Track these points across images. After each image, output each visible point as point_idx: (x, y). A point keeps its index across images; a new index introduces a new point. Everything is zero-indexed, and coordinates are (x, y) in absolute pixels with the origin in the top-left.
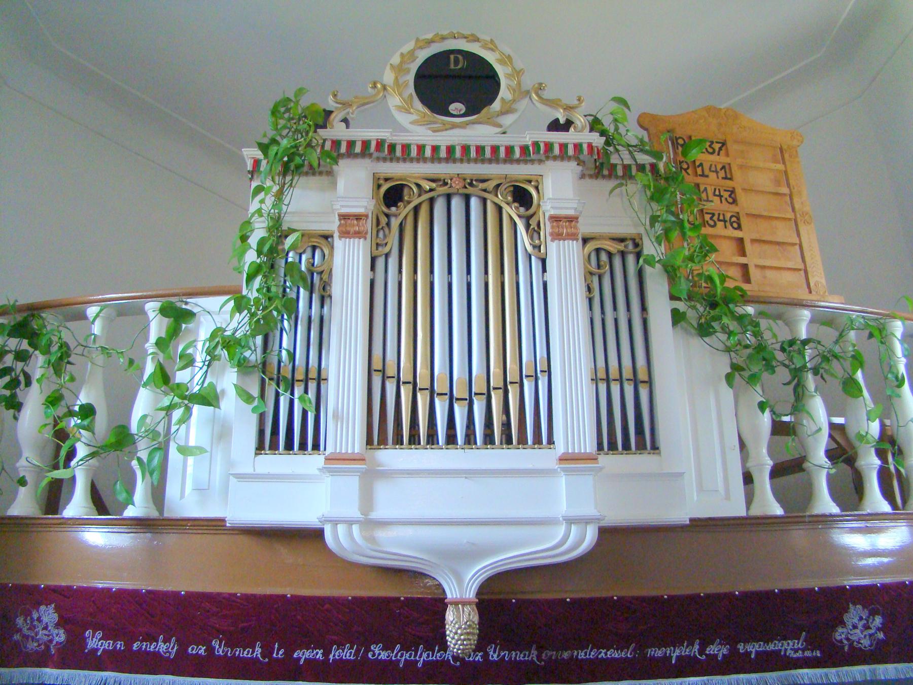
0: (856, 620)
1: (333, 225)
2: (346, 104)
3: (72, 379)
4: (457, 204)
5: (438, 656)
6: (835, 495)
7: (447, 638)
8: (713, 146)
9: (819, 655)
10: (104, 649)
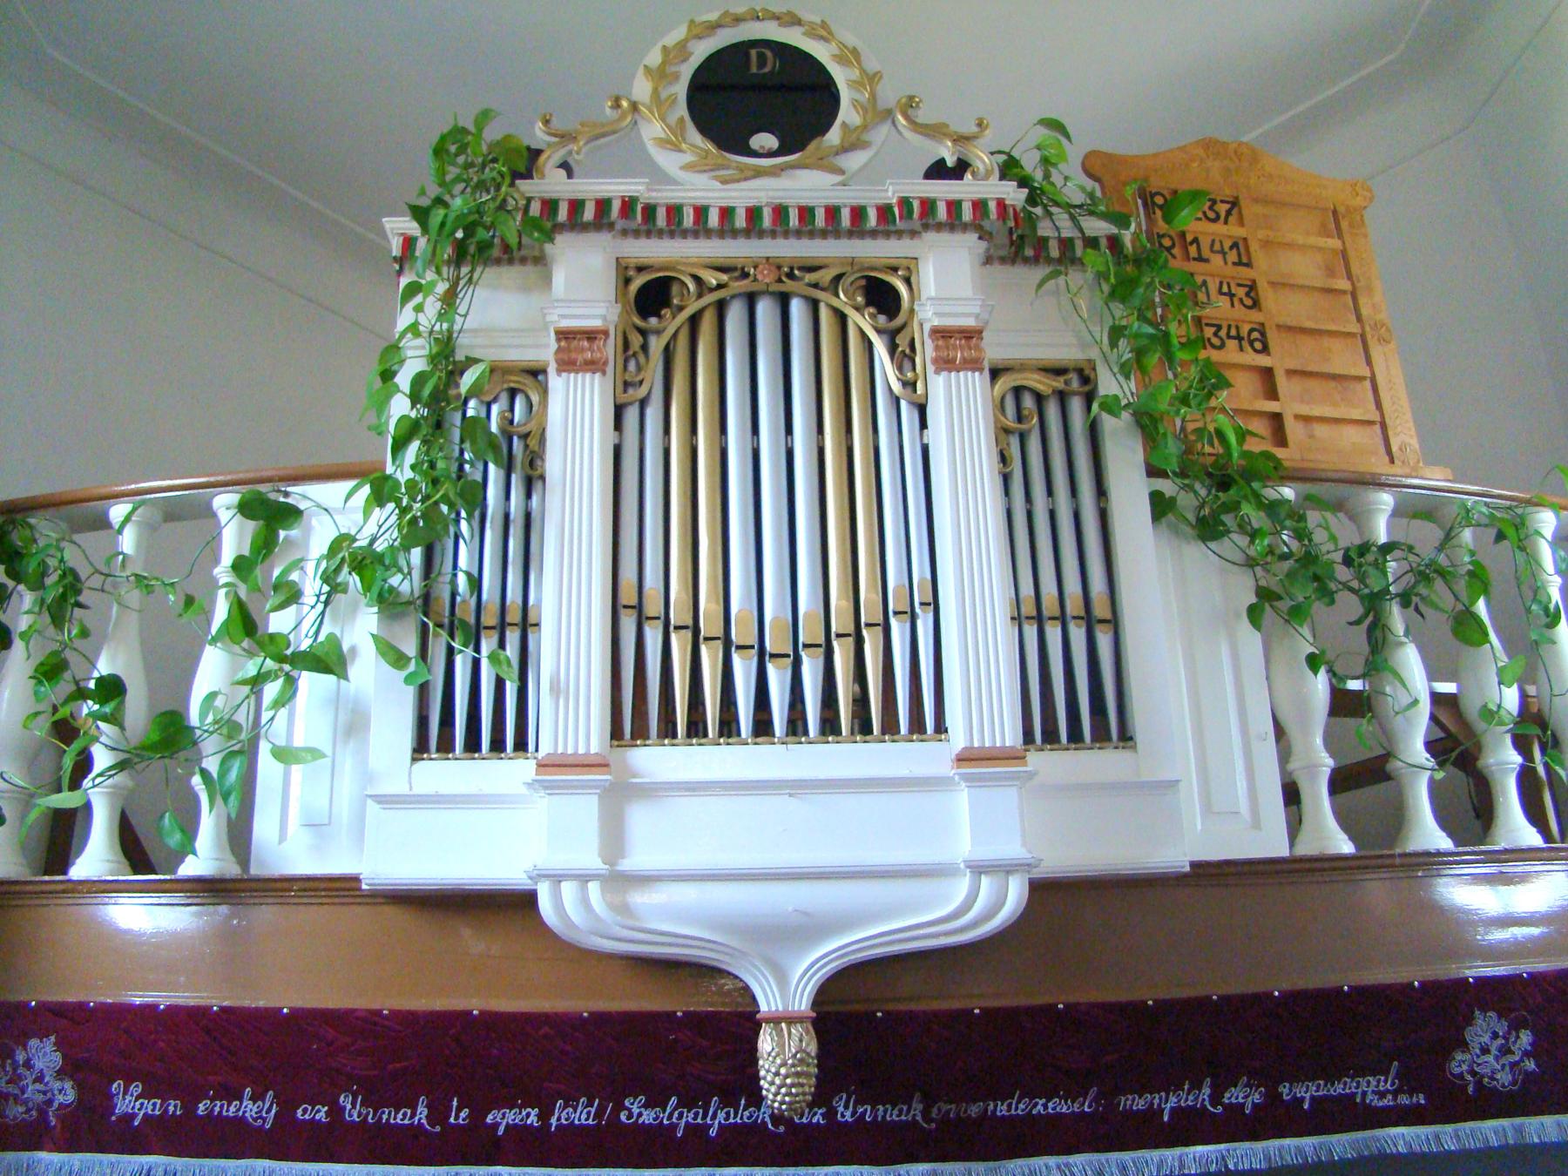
0: (1486, 1039)
1: (545, 352)
2: (566, 137)
3: (85, 633)
5: (744, 1115)
7: (762, 1082)
8: (1216, 207)
9: (1423, 1102)
10: (145, 1114)
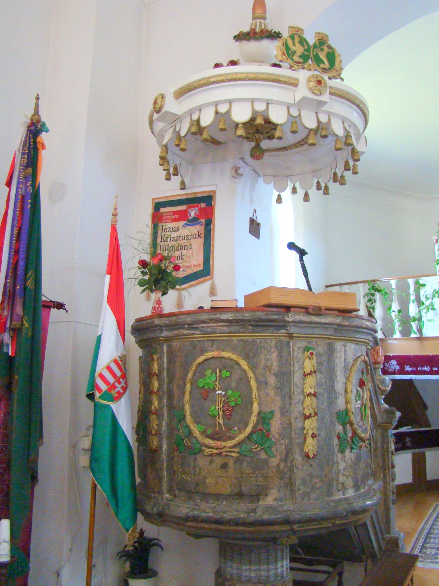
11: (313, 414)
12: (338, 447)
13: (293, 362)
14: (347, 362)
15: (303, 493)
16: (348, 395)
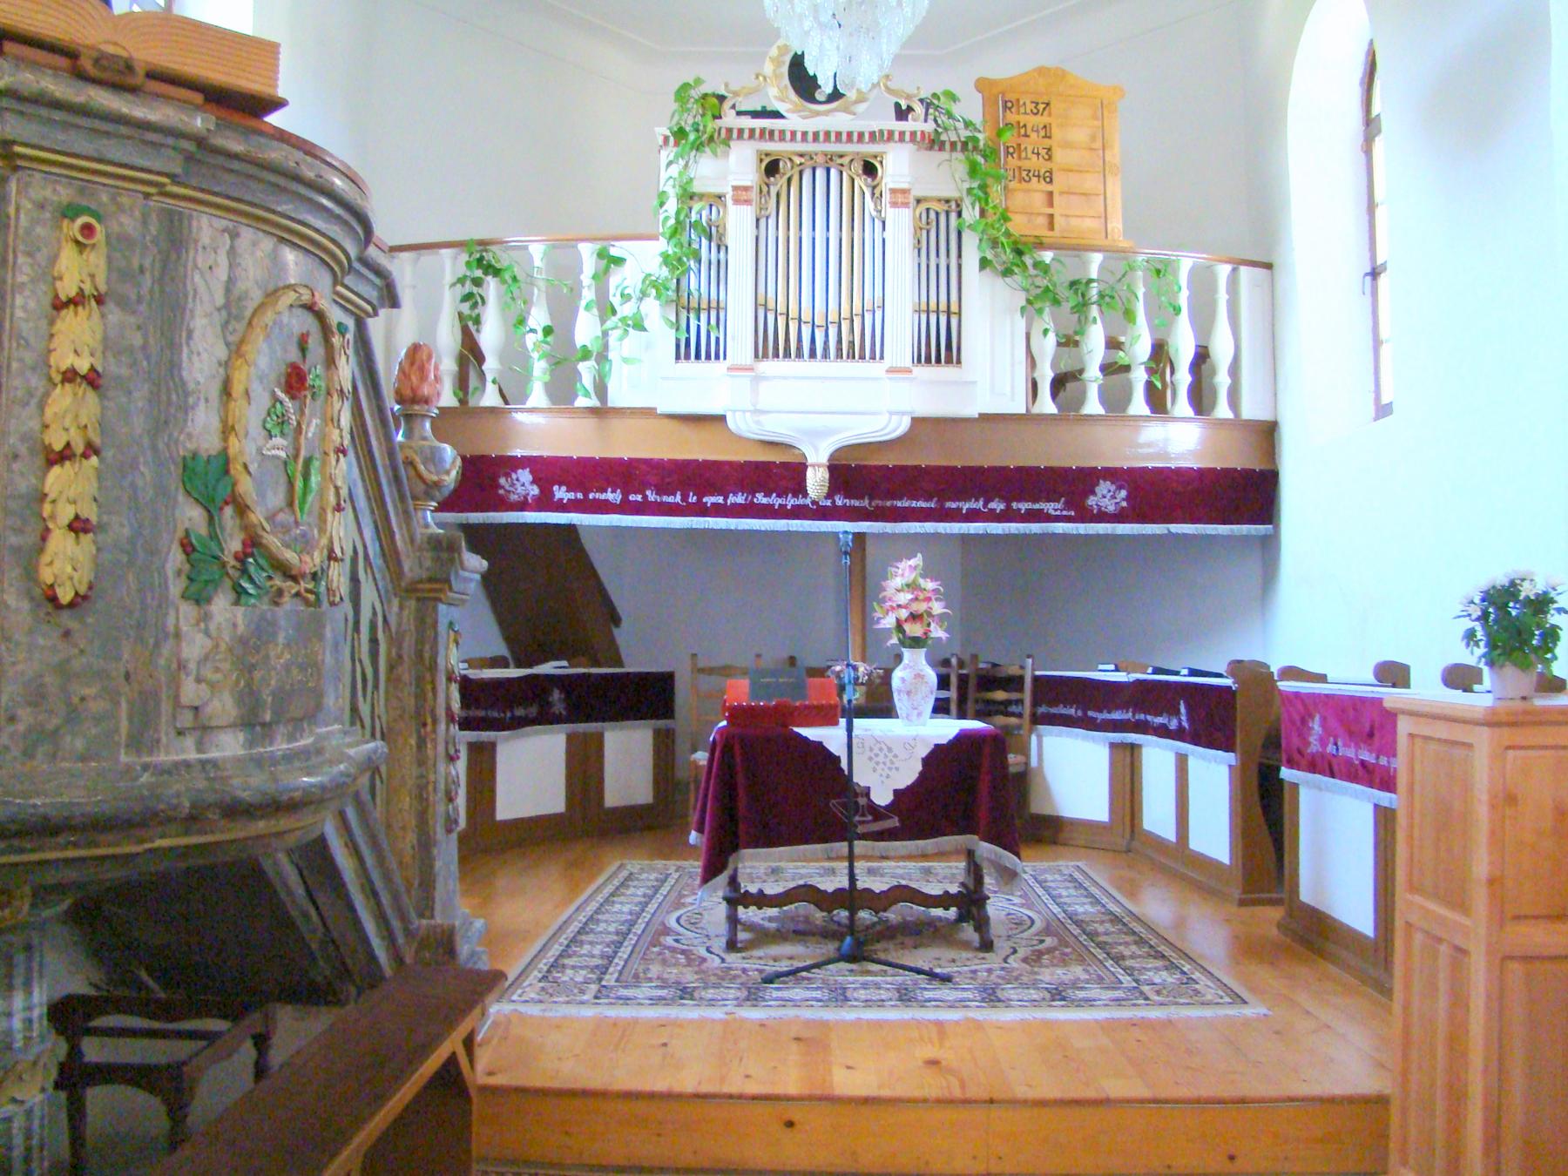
0: (1105, 492)
4: (820, 173)
5: (801, 501)
6: (1103, 400)
11: (79, 448)
12: (183, 582)
13: (14, 252)
14: (236, 292)
15: (29, 730)
16: (232, 405)
